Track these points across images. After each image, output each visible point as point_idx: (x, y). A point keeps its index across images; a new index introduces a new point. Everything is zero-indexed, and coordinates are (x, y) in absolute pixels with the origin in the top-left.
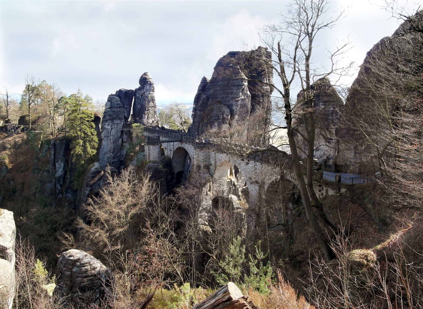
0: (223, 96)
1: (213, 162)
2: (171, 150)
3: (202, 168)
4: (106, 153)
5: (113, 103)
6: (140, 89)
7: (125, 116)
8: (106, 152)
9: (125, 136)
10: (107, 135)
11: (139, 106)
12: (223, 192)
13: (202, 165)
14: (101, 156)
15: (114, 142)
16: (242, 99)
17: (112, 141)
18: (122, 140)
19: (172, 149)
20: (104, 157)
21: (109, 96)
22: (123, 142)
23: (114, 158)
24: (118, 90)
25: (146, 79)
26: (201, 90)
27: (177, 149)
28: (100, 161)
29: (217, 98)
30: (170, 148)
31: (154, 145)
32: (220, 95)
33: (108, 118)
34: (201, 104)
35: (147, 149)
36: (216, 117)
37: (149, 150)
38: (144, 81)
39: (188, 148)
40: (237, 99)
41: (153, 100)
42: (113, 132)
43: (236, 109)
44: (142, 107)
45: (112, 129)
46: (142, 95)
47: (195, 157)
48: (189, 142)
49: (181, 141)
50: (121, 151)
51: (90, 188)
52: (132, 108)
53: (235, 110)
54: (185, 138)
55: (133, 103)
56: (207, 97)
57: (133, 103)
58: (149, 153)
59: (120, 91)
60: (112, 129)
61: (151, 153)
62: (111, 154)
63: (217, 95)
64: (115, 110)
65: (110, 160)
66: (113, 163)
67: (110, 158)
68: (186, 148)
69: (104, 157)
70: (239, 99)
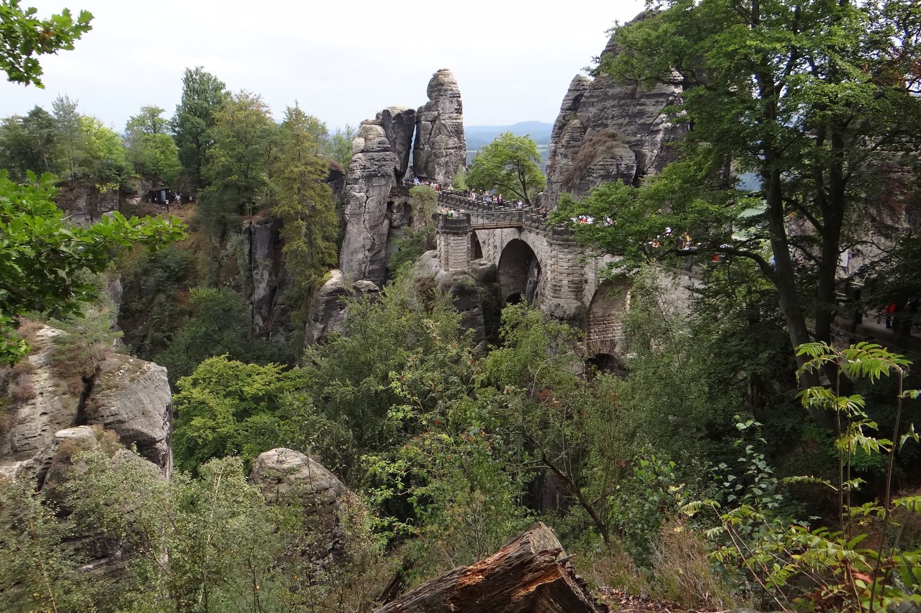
0: (621, 121)
1: (590, 276)
2: (495, 247)
3: (565, 289)
6: (428, 107)
7: (395, 169)
10: (358, 211)
12: (613, 344)
14: (344, 257)
15: (372, 228)
16: (666, 129)
17: (367, 226)
18: (391, 223)
19: (498, 244)
20: (351, 260)
21: (362, 124)
22: (391, 227)
23: (372, 262)
24: (380, 110)
26: (569, 109)
27: (509, 244)
29: (606, 126)
30: (495, 241)
31: (457, 234)
32: (613, 118)
34: (568, 142)
35: (443, 243)
36: (602, 172)
38: (438, 87)
40: (656, 129)
41: (458, 131)
42: (371, 204)
45: (368, 198)
46: (433, 121)
48: (537, 228)
51: (322, 326)
53: (649, 154)
54: (527, 220)
56: (582, 124)
59: (386, 113)
60: (368, 198)
62: (367, 252)
63: (607, 118)
64: (375, 155)
65: (364, 266)
66: (370, 272)
68: (529, 243)
70: (661, 127)
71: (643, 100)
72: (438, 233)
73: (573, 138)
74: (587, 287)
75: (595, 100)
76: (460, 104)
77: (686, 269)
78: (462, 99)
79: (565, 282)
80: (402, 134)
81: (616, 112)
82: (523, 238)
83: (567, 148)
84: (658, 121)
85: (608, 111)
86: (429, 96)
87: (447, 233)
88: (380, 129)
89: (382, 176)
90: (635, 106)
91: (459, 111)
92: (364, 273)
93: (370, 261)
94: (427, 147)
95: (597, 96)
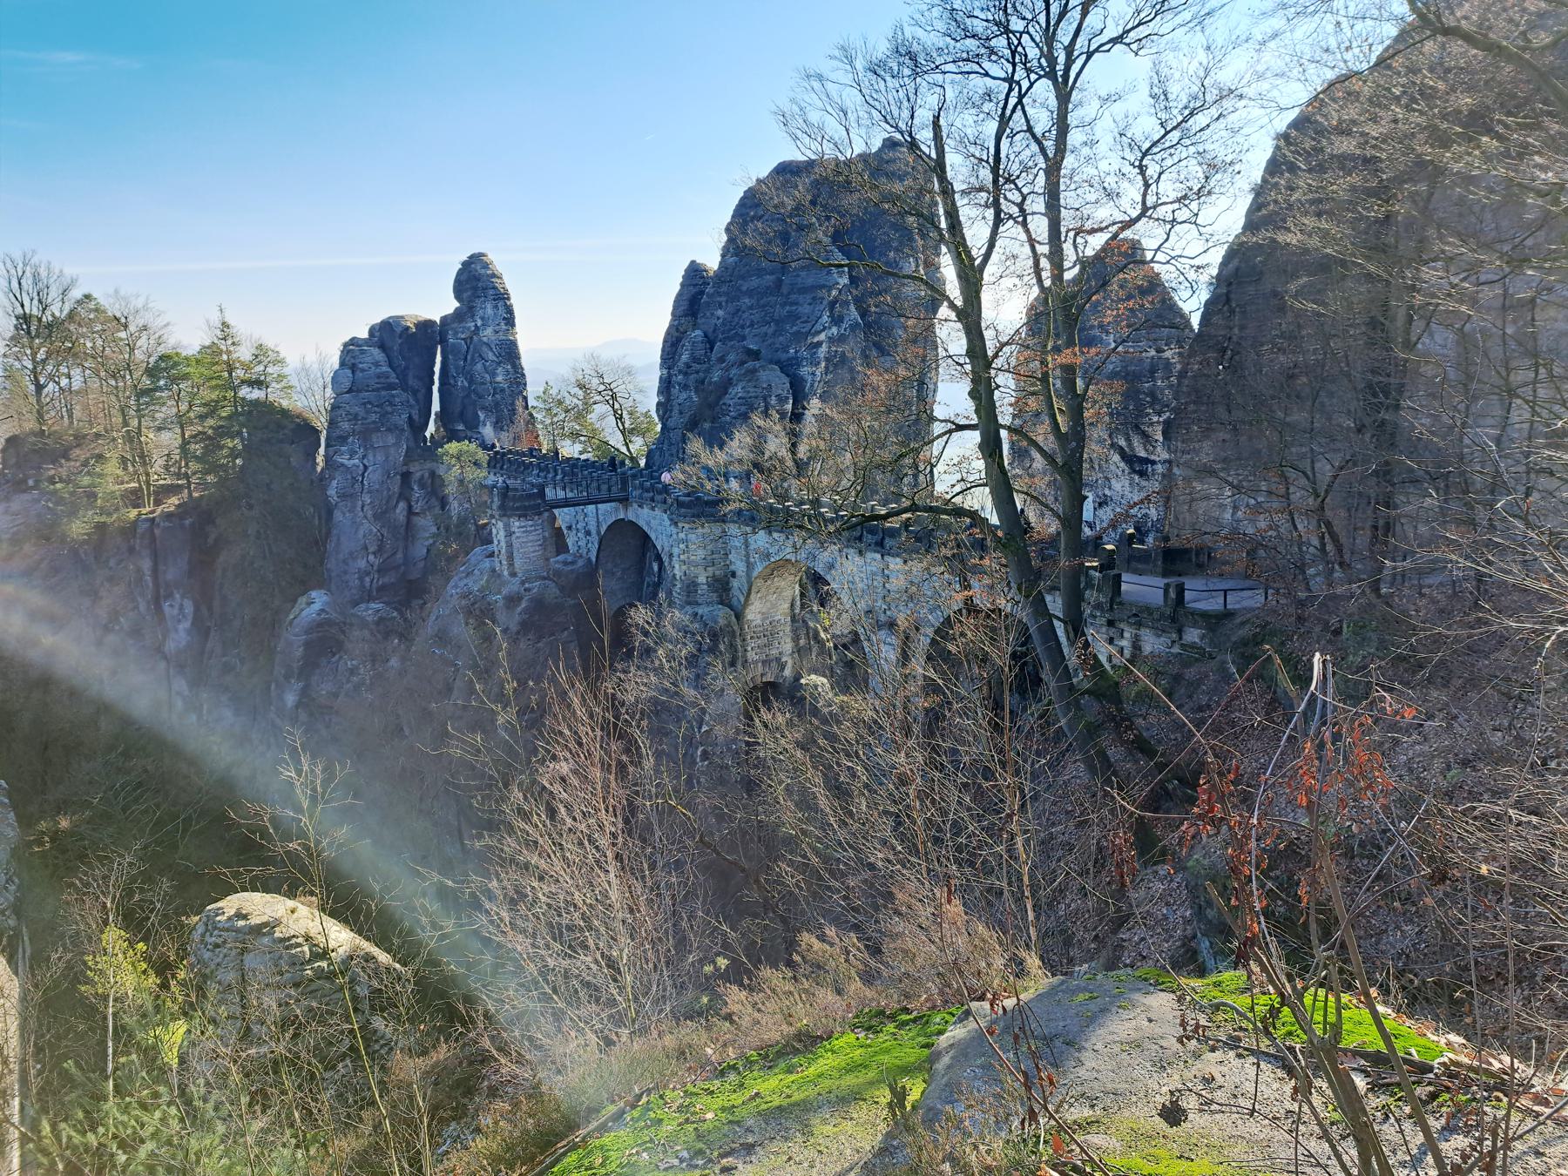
1: (739, 567)
2: (588, 533)
4: (352, 556)
5: (363, 370)
6: (458, 316)
8: (351, 554)
9: (417, 493)
11: (462, 382)
12: (783, 667)
13: (702, 579)
16: (831, 340)
18: (410, 507)
19: (594, 532)
21: (346, 345)
25: (477, 278)
28: (333, 587)
29: (744, 338)
30: (584, 525)
31: (525, 516)
32: (752, 325)
33: (346, 426)
35: (502, 533)
37: (509, 534)
39: (648, 524)
41: (510, 353)
42: (374, 476)
43: (813, 374)
44: (471, 381)
45: (366, 468)
46: (469, 341)
47: (676, 551)
49: (624, 501)
50: (406, 548)
52: (435, 388)
53: (810, 379)
54: (635, 488)
55: (437, 369)
57: (437, 369)
58: (510, 545)
60: (366, 468)
61: (516, 544)
62: (371, 557)
63: (743, 327)
66: (381, 589)
67: (368, 574)
68: (642, 523)
69: (345, 572)
70: (822, 337)
71: (793, 297)
72: (492, 516)
73: (695, 359)
74: (735, 583)
75: (723, 299)
76: (509, 310)
77: (877, 544)
78: (515, 301)
79: (702, 579)
80: (416, 360)
81: (756, 316)
82: (631, 516)
83: (686, 374)
84: (819, 327)
85: (746, 315)
86: (458, 296)
87: (509, 517)
88: (377, 353)
89: (389, 430)
90: (783, 305)
91: (510, 321)
92: (370, 591)
93: (379, 571)
94: (462, 382)
95: (726, 294)
